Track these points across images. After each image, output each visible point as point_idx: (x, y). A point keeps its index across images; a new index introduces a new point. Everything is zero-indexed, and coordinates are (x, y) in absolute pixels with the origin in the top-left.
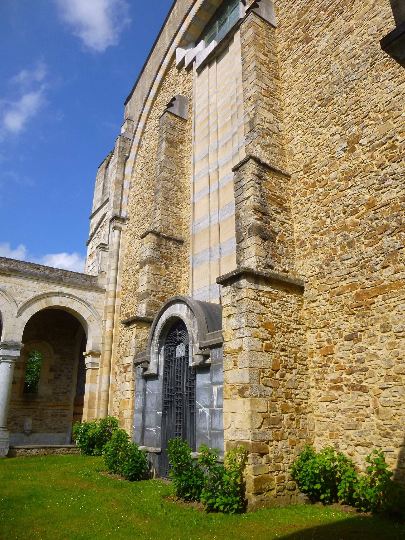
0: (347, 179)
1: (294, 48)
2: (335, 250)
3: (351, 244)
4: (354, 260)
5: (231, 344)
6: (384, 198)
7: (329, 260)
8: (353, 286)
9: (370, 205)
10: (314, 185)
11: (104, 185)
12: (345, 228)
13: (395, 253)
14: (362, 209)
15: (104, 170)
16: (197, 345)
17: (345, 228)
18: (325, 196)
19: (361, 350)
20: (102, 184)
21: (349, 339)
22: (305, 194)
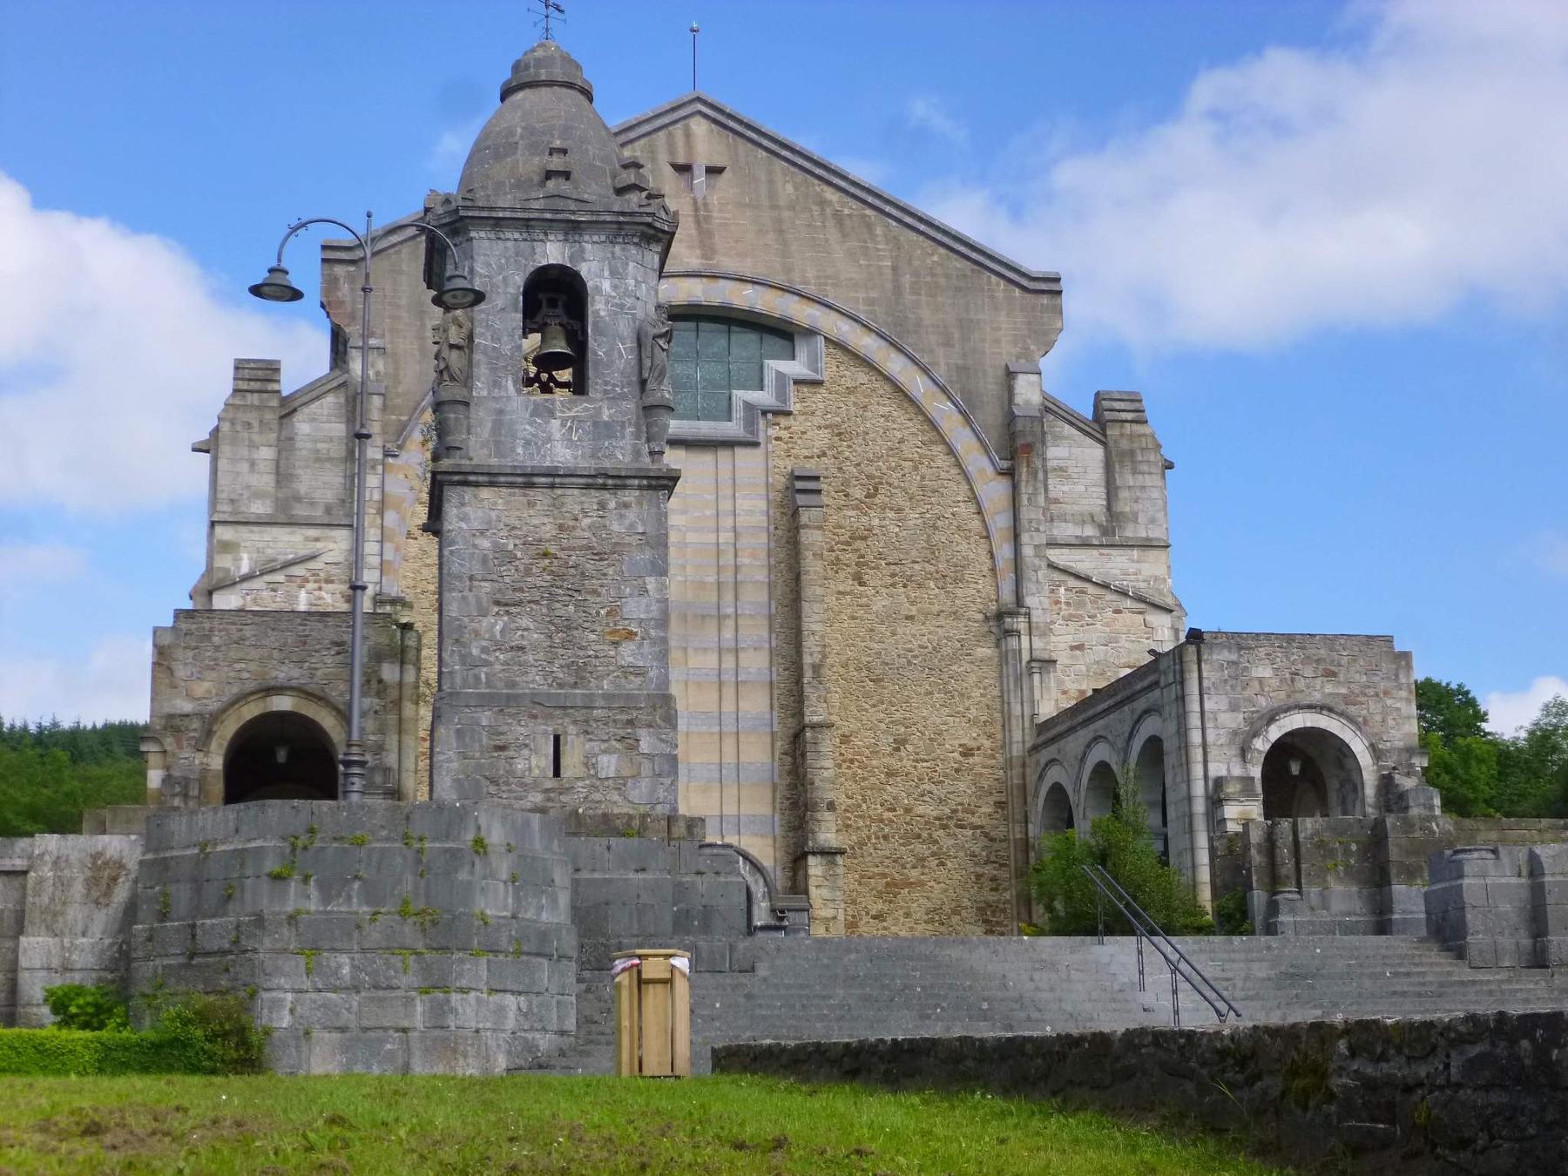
0: (889, 775)
1: (842, 575)
2: (869, 838)
3: (885, 837)
4: (887, 853)
5: (822, 911)
6: (920, 810)
7: (861, 844)
8: (884, 875)
9: (908, 810)
10: (852, 761)
11: (278, 462)
12: (882, 821)
13: (923, 859)
14: (900, 811)
15: (270, 417)
16: (765, 905)
17: (882, 821)
18: (864, 779)
19: (885, 928)
20: (266, 454)
21: (874, 917)
22: (839, 766)
